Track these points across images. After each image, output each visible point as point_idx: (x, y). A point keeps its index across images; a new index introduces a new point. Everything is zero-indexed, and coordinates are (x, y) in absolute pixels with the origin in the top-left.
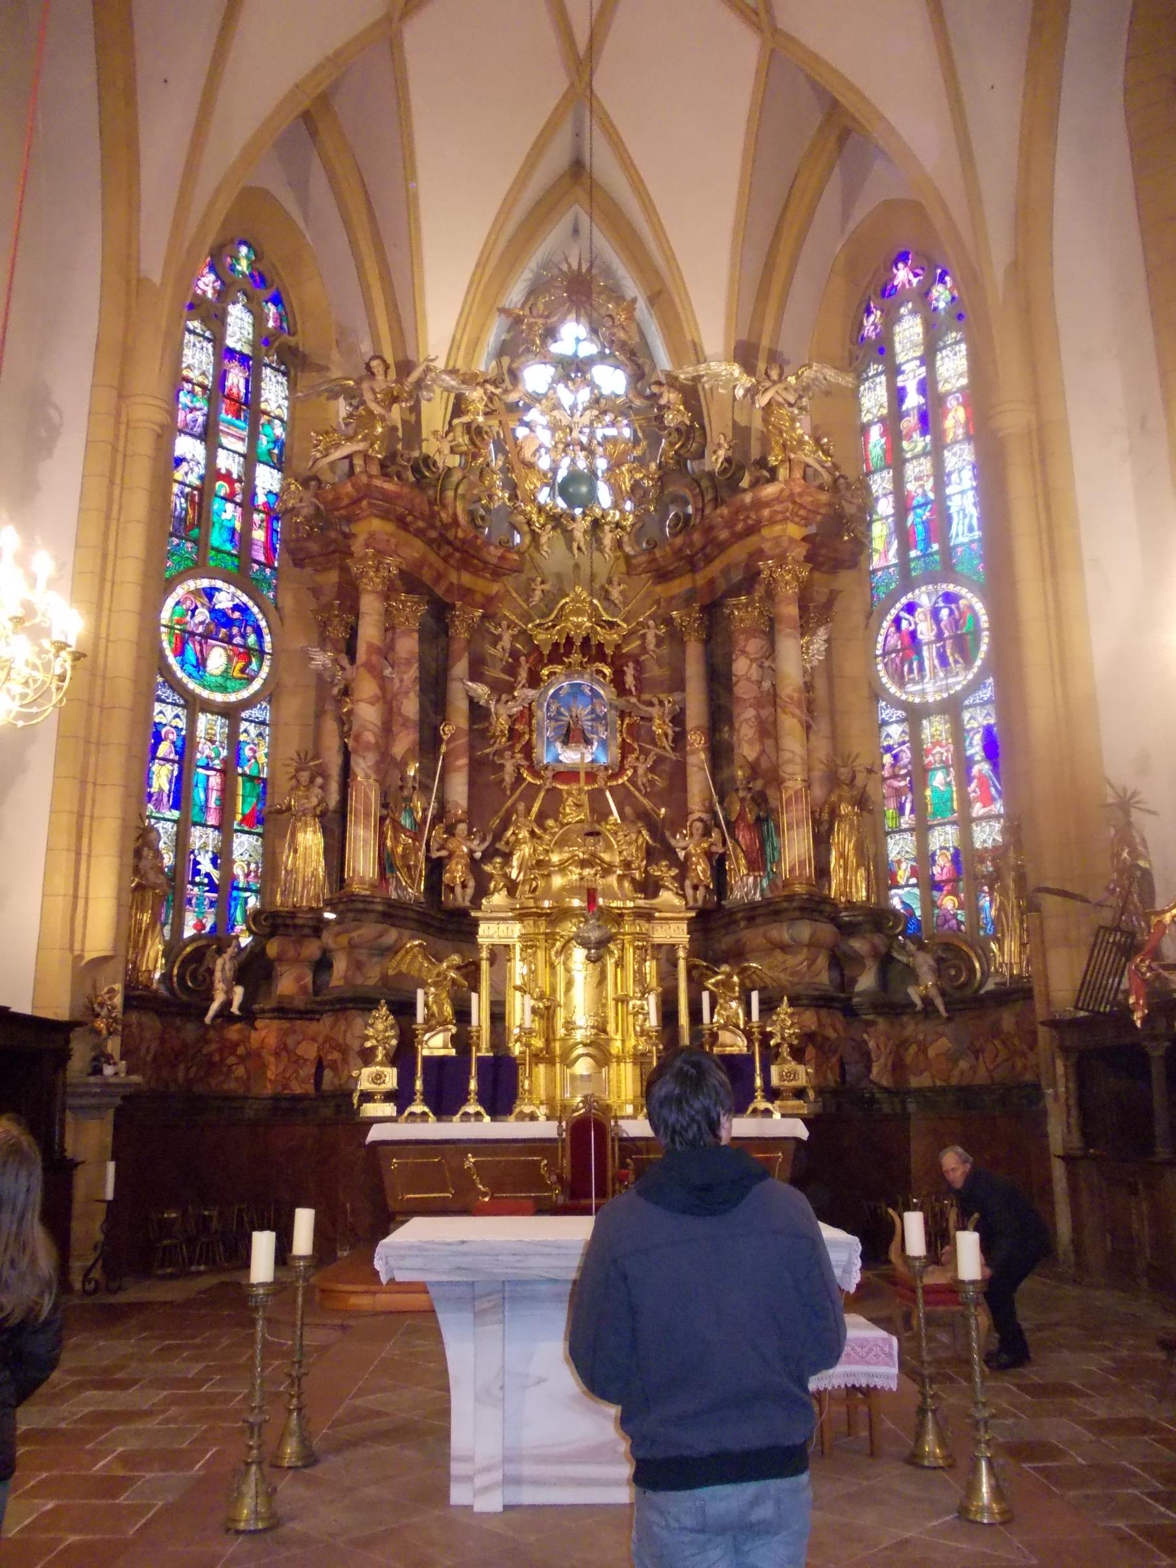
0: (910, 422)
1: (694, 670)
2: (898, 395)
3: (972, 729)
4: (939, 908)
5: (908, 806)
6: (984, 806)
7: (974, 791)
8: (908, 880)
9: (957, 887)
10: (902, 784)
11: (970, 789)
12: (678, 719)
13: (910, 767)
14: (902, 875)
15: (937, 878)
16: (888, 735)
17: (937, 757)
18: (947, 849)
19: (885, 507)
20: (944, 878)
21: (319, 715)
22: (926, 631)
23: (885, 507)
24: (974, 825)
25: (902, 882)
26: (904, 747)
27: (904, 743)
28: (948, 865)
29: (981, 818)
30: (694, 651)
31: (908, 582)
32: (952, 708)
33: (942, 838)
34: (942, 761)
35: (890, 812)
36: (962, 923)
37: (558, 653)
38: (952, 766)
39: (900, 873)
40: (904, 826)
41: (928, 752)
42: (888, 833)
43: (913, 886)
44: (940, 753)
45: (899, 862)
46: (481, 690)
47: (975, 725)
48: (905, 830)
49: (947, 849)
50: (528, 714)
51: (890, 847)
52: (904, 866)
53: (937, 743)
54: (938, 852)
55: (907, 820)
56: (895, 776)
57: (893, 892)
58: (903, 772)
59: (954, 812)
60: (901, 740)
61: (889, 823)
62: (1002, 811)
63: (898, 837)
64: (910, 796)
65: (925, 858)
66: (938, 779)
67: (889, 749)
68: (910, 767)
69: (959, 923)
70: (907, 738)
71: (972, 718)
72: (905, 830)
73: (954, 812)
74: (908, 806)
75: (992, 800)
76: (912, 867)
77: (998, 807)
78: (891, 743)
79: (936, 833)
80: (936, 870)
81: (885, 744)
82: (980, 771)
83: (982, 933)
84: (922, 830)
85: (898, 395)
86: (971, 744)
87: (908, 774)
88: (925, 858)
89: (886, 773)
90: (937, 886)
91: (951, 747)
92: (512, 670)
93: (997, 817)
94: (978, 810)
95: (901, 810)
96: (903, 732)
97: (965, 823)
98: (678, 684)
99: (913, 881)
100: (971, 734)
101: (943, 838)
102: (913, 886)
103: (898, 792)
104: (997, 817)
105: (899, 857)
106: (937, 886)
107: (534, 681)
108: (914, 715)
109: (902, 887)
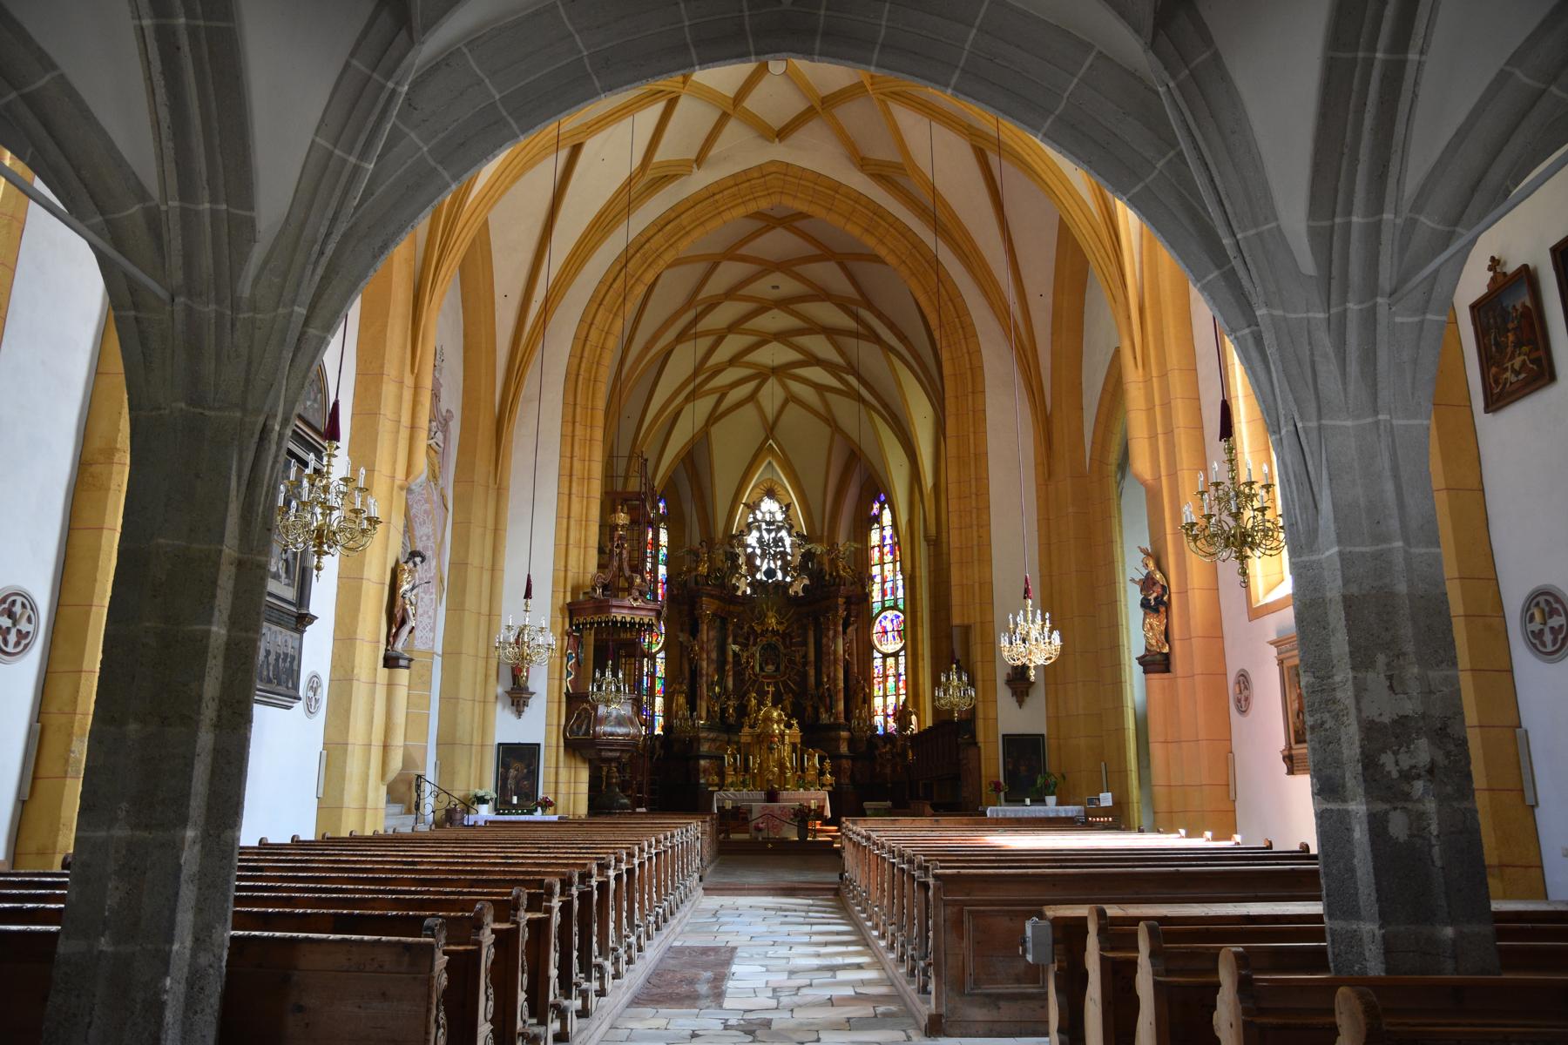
0: (887, 549)
1: (811, 641)
2: (883, 538)
12: (805, 656)
19: (878, 579)
21: (681, 656)
22: (889, 628)
23: (878, 579)
30: (811, 634)
31: (884, 609)
32: (895, 655)
37: (762, 634)
44: (891, 672)
46: (736, 648)
50: (753, 656)
65: (885, 707)
85: (883, 538)
88: (885, 707)
92: (747, 639)
98: (805, 644)
107: (755, 644)
108: (885, 656)
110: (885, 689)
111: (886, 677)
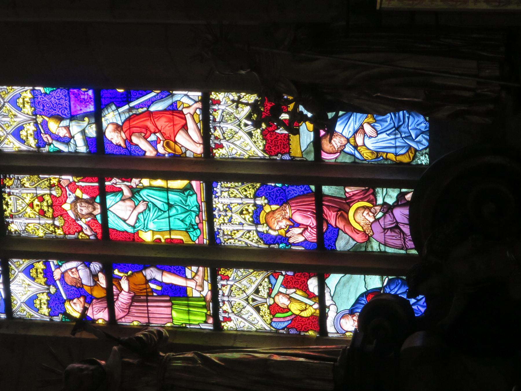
3: (37, 135)
4: (368, 239)
5: (169, 279)
6: (185, 127)
7: (154, 144)
8: (310, 295)
9: (332, 198)
10: (125, 284)
11: (150, 153)
13: (96, 266)
14: (301, 306)
15: (311, 236)
16: (31, 302)
17: (83, 209)
18: (259, 209)
20: (312, 222)
24: (218, 153)
25: (312, 309)
26: (57, 275)
27: (48, 273)
28: (288, 212)
29: (206, 135)
33: (237, 219)
34: (91, 202)
35: (179, 317)
36: (401, 196)
38: (102, 183)
39: (295, 308)
40: (207, 292)
41: (71, 224)
42: (217, 323)
43: (322, 286)
45: (274, 309)
47: (31, 128)
48: (215, 291)
49: (259, 209)
51: (244, 326)
52: (282, 301)
53: (56, 205)
54: (263, 228)
55: (195, 281)
56: (110, 300)
57: (330, 329)
58: (102, 281)
59: (190, 187)
60: (42, 279)
61: (199, 320)
62: (197, 95)
63: (226, 307)
64: (151, 273)
65: (270, 258)
66: (122, 214)
67: (56, 302)
68: (96, 266)
69: (400, 201)
70: (40, 266)
71: (16, 134)
72: (215, 291)
73: (190, 187)
74: (169, 279)
75: (174, 110)
76: (286, 284)
77: (188, 100)
78: (44, 298)
79: (227, 228)
80: (296, 236)
81: (45, 310)
82: (118, 128)
83: (424, 160)
84: (216, 257)
86: (66, 141)
87: (107, 271)
88: (270, 258)
89: (100, 315)
90: (325, 237)
91: (67, 179)
93: (206, 104)
94: (190, 143)
95: (177, 293)
96: (27, 271)
97: (210, 170)
99: (313, 284)
100: (46, 137)
101: (238, 215)
102: (322, 286)
103: (141, 296)
104: (206, 104)
105: (264, 309)
106: (325, 237)
109: (323, 307)
110: (173, 255)
111: (114, 252)
